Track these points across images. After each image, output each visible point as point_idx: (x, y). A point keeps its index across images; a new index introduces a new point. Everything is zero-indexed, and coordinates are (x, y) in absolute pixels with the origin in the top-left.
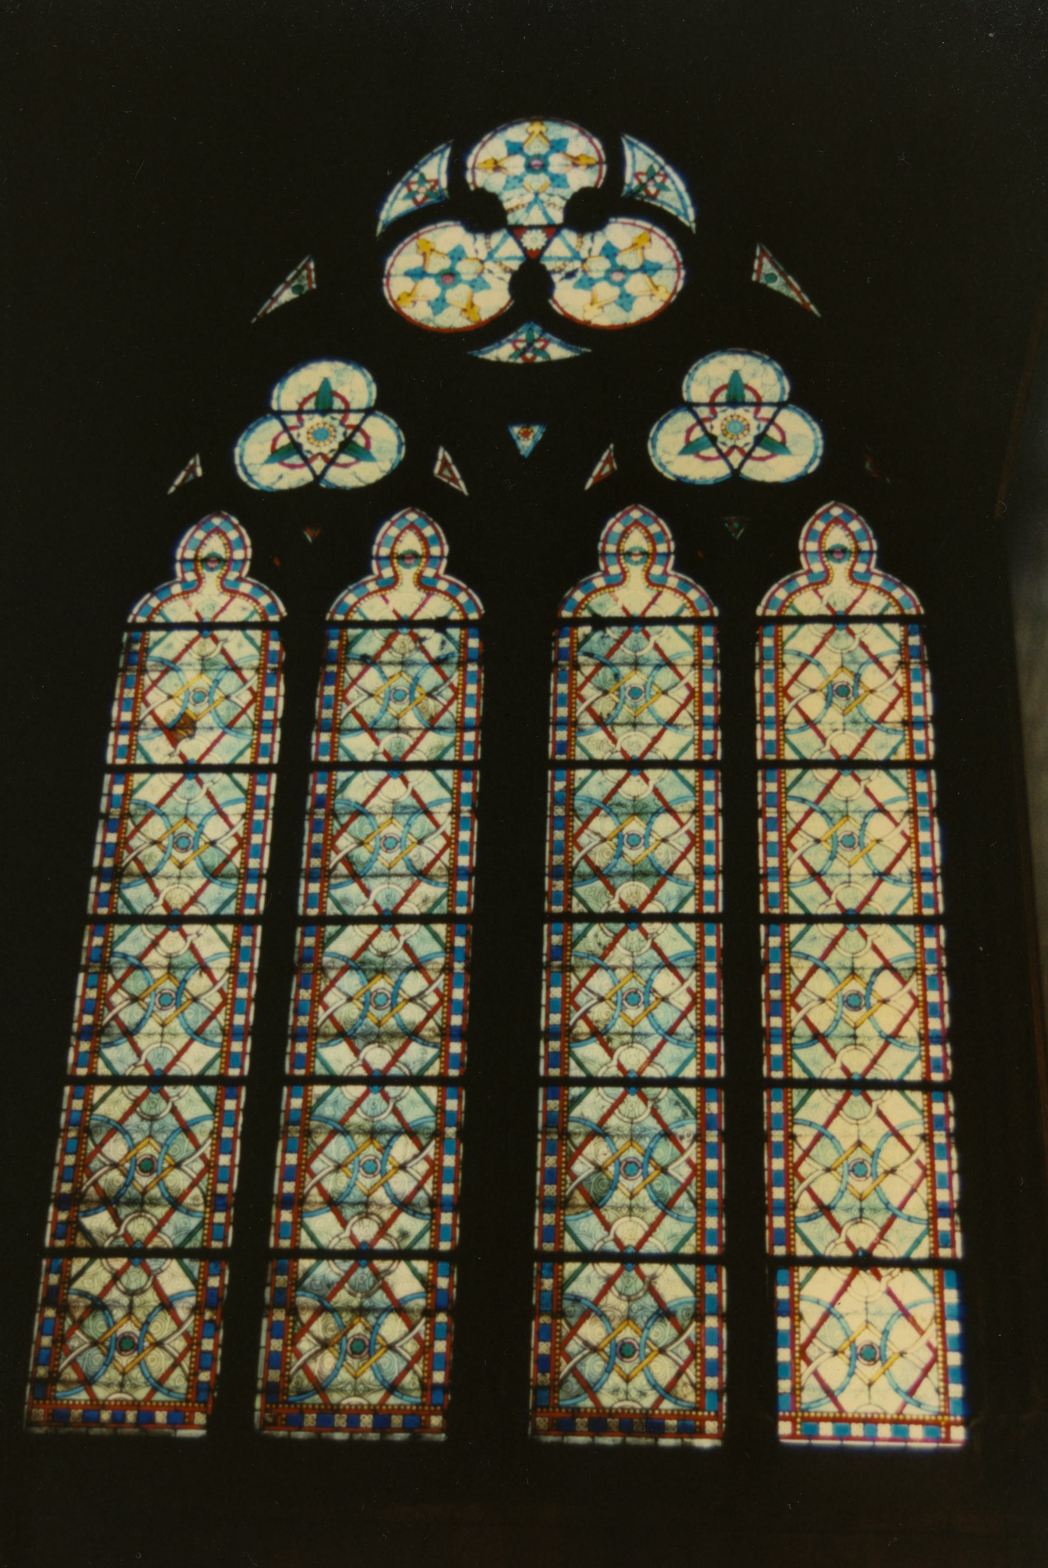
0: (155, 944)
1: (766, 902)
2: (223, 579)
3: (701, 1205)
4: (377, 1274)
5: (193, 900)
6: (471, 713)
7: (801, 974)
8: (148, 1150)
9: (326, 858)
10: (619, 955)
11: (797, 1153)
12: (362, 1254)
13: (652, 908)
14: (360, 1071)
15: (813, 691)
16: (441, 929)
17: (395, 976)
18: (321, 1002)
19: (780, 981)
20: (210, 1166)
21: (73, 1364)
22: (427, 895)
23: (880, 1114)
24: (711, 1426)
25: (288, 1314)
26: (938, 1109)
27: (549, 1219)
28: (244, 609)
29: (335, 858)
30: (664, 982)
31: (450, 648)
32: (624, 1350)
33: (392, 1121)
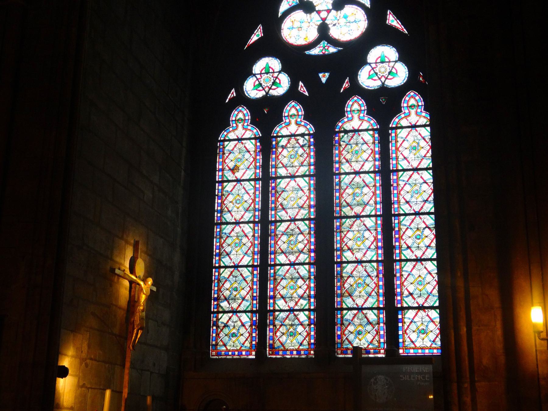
0: (233, 230)
2: (243, 125)
3: (378, 295)
4: (295, 315)
5: (242, 217)
7: (404, 230)
8: (235, 285)
9: (275, 204)
10: (355, 227)
11: (403, 279)
12: (291, 310)
13: (363, 214)
14: (288, 262)
15: (406, 149)
16: (307, 222)
18: (277, 244)
20: (252, 289)
21: (221, 340)
22: (303, 213)
23: (425, 268)
27: (339, 299)
29: (278, 204)
30: (367, 234)
31: (306, 142)
32: (359, 333)
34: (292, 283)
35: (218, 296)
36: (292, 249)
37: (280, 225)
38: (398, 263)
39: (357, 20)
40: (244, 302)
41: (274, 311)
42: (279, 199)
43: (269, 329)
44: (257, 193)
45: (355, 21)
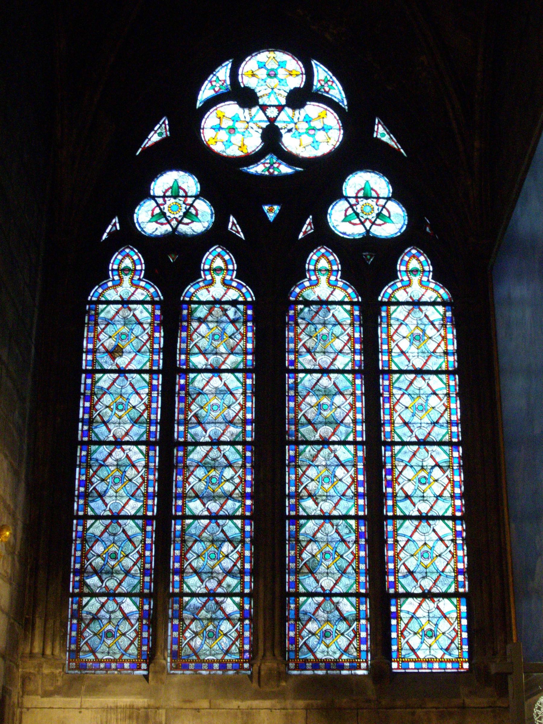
0: (110, 454)
1: (384, 436)
2: (132, 279)
3: (357, 572)
4: (217, 602)
5: (127, 434)
6: (250, 346)
8: (113, 549)
9: (186, 415)
10: (320, 460)
11: (399, 548)
12: (211, 595)
13: (334, 438)
14: (206, 513)
15: (404, 337)
16: (240, 448)
17: (220, 470)
19: (391, 472)
20: (142, 556)
21: (86, 643)
24: (363, 665)
25: (180, 621)
26: (459, 528)
27: (292, 578)
28: (143, 294)
29: (190, 415)
30: (340, 472)
31: (239, 314)
32: (325, 634)
33: (222, 535)
34: (212, 549)
35: (82, 567)
36: (214, 491)
37: (193, 450)
38: (390, 521)
39: (325, 127)
40: (128, 579)
41: (182, 594)
42: (193, 407)
43: (173, 626)
44: (155, 394)
45: (323, 129)
